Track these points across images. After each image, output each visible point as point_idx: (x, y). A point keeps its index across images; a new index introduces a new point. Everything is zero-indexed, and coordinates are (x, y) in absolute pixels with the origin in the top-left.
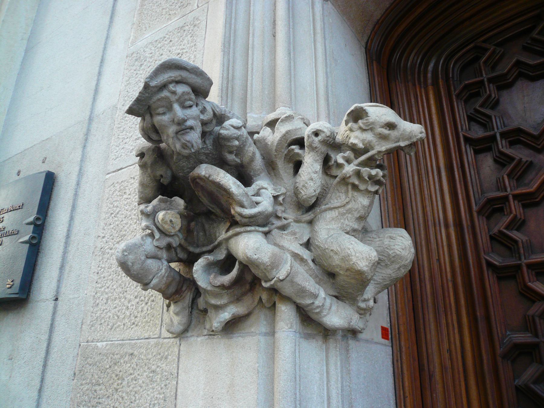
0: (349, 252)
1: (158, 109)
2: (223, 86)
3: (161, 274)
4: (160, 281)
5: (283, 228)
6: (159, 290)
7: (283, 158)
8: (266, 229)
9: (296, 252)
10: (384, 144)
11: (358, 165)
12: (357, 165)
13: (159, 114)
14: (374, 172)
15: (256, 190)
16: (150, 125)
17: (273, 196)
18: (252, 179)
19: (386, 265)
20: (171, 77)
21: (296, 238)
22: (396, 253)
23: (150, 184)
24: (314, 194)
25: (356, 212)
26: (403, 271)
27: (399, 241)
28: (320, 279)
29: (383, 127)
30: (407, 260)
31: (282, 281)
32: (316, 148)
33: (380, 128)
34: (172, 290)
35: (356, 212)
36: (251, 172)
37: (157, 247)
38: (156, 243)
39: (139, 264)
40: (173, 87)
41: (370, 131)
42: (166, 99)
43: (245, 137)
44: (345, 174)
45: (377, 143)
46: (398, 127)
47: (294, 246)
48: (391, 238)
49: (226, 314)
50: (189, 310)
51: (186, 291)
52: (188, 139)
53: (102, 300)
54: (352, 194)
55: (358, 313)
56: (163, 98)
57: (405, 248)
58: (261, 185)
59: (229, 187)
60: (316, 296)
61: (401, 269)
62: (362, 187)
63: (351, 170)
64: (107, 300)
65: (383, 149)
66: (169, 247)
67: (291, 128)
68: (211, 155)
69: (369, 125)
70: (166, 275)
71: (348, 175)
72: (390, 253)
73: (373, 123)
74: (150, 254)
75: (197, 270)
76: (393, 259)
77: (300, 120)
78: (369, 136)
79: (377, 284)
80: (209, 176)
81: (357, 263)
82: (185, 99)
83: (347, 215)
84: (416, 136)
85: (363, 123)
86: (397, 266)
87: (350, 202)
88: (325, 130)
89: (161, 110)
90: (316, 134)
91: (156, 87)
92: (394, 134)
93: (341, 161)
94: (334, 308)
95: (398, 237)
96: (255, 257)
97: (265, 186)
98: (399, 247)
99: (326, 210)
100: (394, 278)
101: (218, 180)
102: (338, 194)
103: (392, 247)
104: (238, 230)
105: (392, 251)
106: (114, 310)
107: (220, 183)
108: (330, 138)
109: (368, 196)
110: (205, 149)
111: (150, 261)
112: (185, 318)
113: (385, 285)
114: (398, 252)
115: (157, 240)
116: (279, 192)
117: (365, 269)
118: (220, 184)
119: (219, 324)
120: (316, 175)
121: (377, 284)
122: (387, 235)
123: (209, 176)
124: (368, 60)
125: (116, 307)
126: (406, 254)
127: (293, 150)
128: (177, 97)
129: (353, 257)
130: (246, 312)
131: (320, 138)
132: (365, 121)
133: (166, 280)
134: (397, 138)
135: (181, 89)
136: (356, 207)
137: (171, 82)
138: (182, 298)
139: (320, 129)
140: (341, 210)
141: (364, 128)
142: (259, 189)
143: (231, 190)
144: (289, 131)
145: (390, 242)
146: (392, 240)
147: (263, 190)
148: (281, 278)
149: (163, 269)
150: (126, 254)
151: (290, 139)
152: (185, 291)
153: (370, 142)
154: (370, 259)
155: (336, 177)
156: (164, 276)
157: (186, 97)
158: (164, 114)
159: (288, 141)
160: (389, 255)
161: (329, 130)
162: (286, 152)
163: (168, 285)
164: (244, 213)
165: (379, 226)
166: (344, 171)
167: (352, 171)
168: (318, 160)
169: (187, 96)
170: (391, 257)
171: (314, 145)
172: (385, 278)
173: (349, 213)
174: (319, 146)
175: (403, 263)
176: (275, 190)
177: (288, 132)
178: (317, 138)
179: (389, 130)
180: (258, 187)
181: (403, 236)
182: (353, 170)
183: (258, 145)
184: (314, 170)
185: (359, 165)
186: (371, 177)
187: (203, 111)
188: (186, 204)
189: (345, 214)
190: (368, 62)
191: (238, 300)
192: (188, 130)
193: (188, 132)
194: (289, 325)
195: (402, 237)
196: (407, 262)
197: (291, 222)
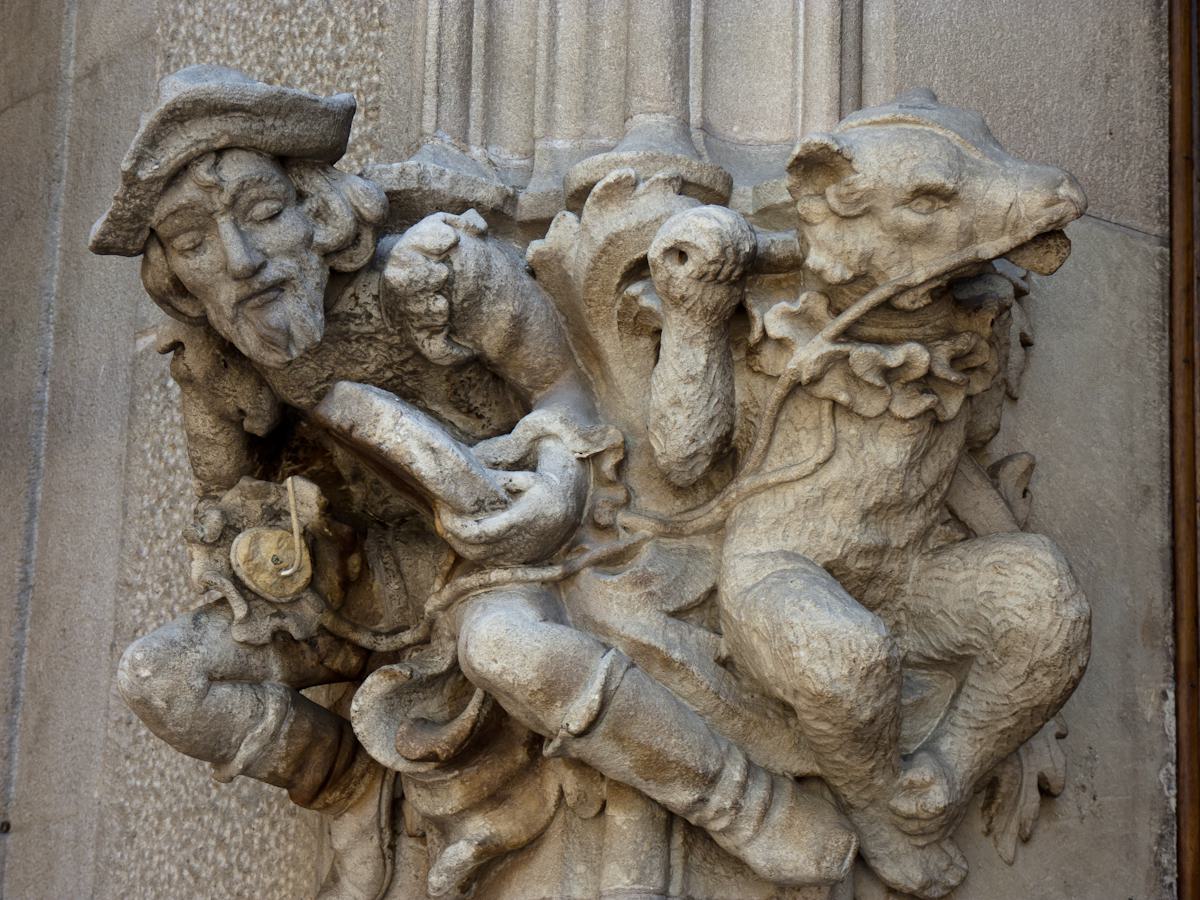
0: (792, 638)
1: (175, 236)
2: (446, 46)
3: (264, 729)
4: (267, 749)
5: (612, 562)
6: (274, 779)
7: (615, 322)
8: (556, 572)
9: (645, 639)
11: (835, 340)
12: (835, 340)
13: (183, 252)
14: (895, 357)
15: (525, 443)
16: (167, 281)
17: (579, 459)
18: (530, 396)
19: (989, 663)
20: (199, 142)
21: (651, 594)
22: (1010, 623)
23: (216, 434)
24: (693, 449)
26: (1048, 682)
27: (1020, 579)
28: (748, 721)
29: (905, 203)
30: (1047, 646)
31: (582, 734)
32: (683, 299)
33: (895, 206)
34: (311, 778)
36: (517, 375)
37: (245, 643)
38: (239, 634)
39: (187, 701)
40: (208, 172)
42: (193, 208)
43: (471, 275)
44: (797, 373)
45: (896, 256)
47: (643, 621)
48: (997, 567)
49: (462, 844)
50: (381, 839)
51: (367, 779)
52: (273, 324)
53: (146, 819)
54: (836, 433)
55: (899, 830)
56: (184, 208)
57: (1037, 602)
58: (539, 426)
59: (407, 459)
60: (710, 780)
61: (1038, 675)
62: (872, 405)
63: (814, 357)
64: (160, 816)
65: (920, 276)
66: (281, 639)
67: (622, 227)
68: (380, 337)
69: (858, 201)
70: (285, 728)
71: (805, 377)
72: (994, 624)
73: (870, 194)
74: (220, 670)
75: (361, 712)
76: (1003, 643)
77: (661, 186)
78: (865, 237)
79: (977, 729)
80: (352, 428)
81: (812, 670)
82: (252, 200)
83: (829, 503)
84: (1030, 219)
85: (839, 196)
86: (1023, 667)
88: (703, 241)
89: (184, 241)
90: (680, 253)
91: (152, 181)
92: (950, 220)
93: (777, 328)
94: (779, 814)
95: (1018, 568)
96: (495, 668)
97: (555, 427)
98: (1020, 601)
99: (754, 492)
100: (1026, 709)
101: (375, 440)
102: (793, 436)
103: (999, 603)
104: (464, 582)
105: (998, 617)
106: (184, 852)
107: (383, 447)
108: (723, 264)
110: (358, 321)
111: (223, 691)
112: (369, 865)
113: (1002, 732)
114: (1016, 621)
115: (242, 622)
116: (598, 445)
117: (841, 687)
118: (381, 451)
119: (444, 878)
120: (691, 389)
121: (977, 729)
122: (987, 560)
123: (352, 428)
125: (186, 844)
126: (1044, 625)
127: (635, 298)
128: (226, 198)
129: (802, 653)
130: (524, 838)
131: (690, 267)
132: (844, 191)
133: (288, 745)
134: (964, 234)
135: (236, 170)
137: (200, 156)
138: (355, 797)
139: (686, 238)
140: (801, 489)
142: (538, 439)
143: (414, 467)
144: (617, 235)
145: (993, 583)
146: (1001, 578)
147: (548, 444)
148: (574, 728)
149: (271, 712)
150: (145, 673)
151: (625, 263)
152: (363, 776)
153: (867, 258)
154: (854, 656)
155: (775, 378)
156: (275, 736)
157: (253, 193)
158: (197, 248)
159: (621, 270)
160: (991, 631)
161: (716, 238)
162: (618, 306)
163: (300, 764)
164: (465, 533)
165: (1147, 490)
166: (791, 365)
167: (816, 362)
168: (696, 336)
169: (255, 190)
170: (997, 636)
171: (677, 293)
172: (997, 708)
173: (835, 497)
174: (691, 292)
175: (1037, 656)
176: (585, 437)
177: (613, 241)
178: (682, 268)
180: (530, 435)
181: (1036, 563)
183: (544, 276)
184: (682, 374)
185: (848, 334)
186: (887, 373)
187: (321, 214)
188: (323, 499)
191: (493, 799)
192: (272, 295)
193: (275, 299)
194: (634, 874)
195: (1028, 564)
196: (1049, 653)
197: (646, 539)
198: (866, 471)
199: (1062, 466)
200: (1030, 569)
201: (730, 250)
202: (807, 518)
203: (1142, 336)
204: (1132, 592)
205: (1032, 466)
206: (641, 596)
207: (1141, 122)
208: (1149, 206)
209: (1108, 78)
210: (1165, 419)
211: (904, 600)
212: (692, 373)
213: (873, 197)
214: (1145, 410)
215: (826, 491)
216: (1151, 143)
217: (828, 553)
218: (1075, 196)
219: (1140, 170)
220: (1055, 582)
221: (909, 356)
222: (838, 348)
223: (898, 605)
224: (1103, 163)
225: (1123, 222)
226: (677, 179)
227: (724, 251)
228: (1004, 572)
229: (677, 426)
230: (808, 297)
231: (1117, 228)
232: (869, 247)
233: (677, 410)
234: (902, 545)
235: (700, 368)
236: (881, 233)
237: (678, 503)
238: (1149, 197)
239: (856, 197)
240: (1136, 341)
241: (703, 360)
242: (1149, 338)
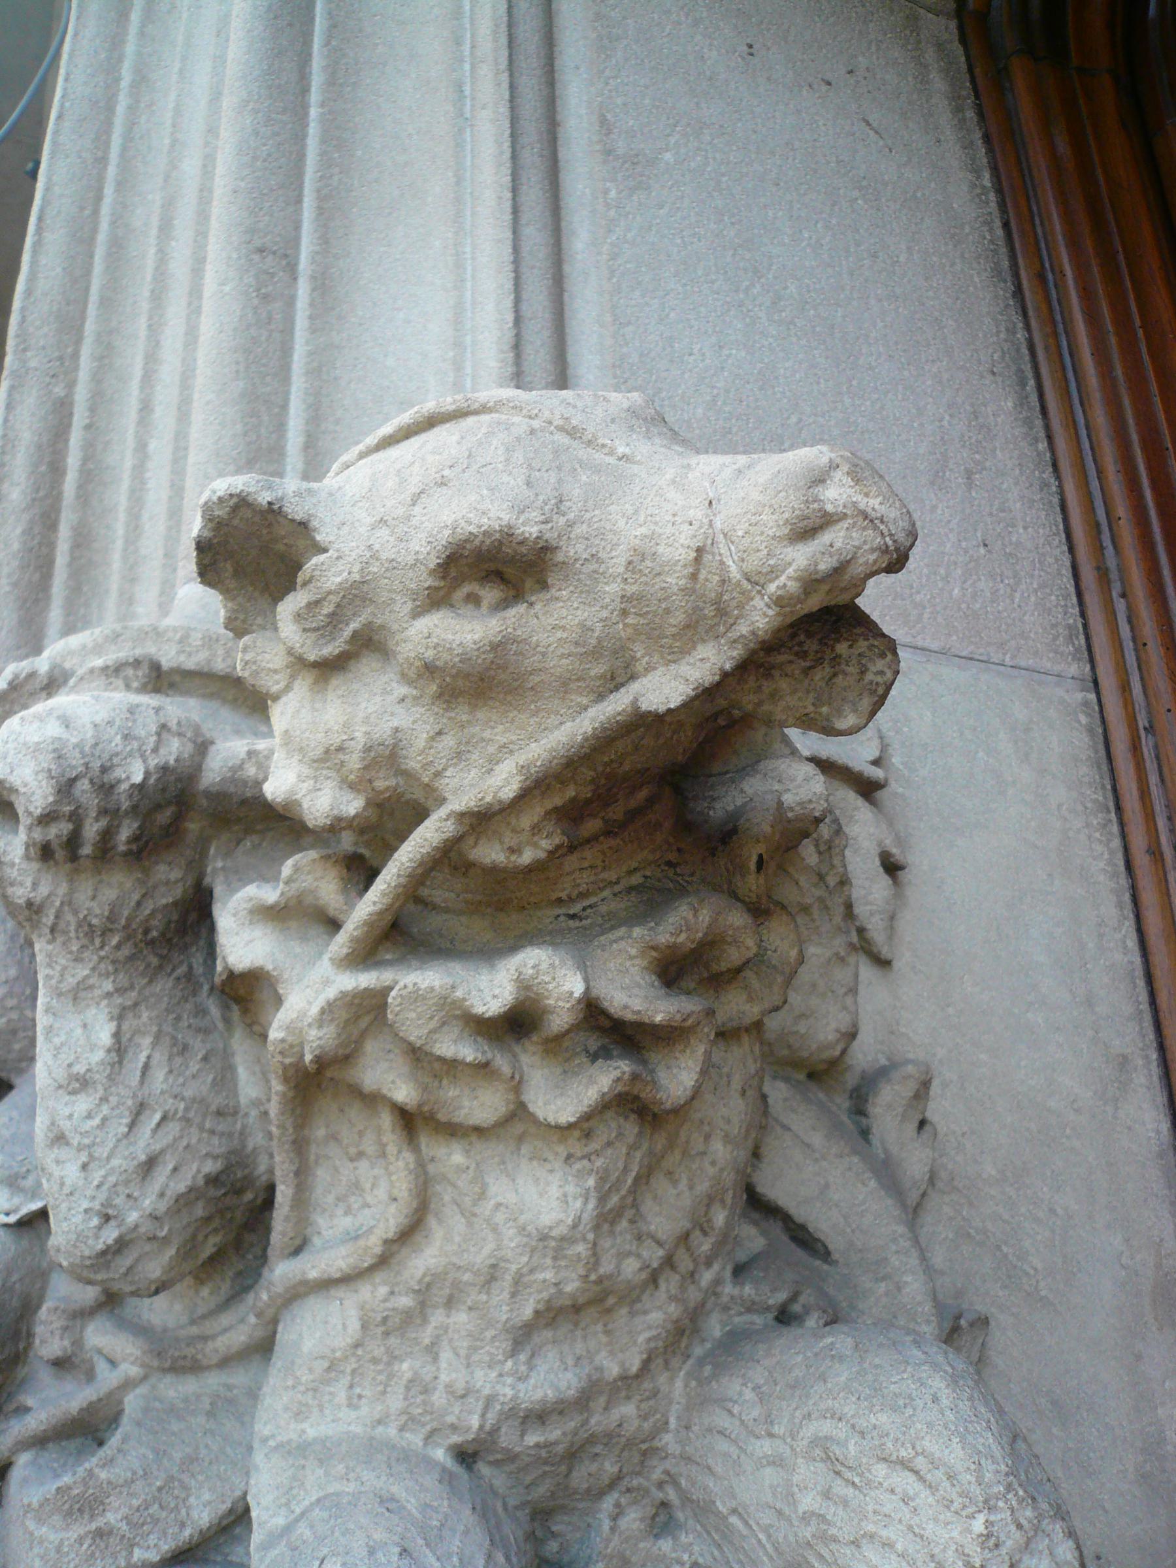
10: (500, 734)
21: (100, 1534)
24: (110, 1235)
25: (501, 1293)
27: (890, 1504)
33: (416, 614)
35: (501, 1293)
41: (367, 665)
45: (449, 742)
46: (573, 550)
69: (335, 620)
83: (437, 1317)
84: (756, 580)
87: (432, 1222)
102: (346, 1170)
109: (562, 1150)
120: (83, 1103)
124: (978, 71)
134: (595, 653)
136: (480, 1257)
141: (330, 650)
146: (840, 1488)
165: (1124, 1062)
167: (320, 1022)
174: (44, 890)
179: (503, 604)
181: (920, 1463)
182: (328, 1010)
189: (411, 1319)
190: (980, 81)
195: (904, 1464)
198: (499, 1248)
199: (983, 1057)
200: (911, 1478)
201: (84, 785)
202: (393, 1358)
203: (1078, 823)
204: (1127, 1240)
205: (926, 1084)
206: (80, 1540)
207: (1025, 528)
208: (1055, 638)
209: (969, 474)
210: (1132, 943)
211: (668, 1465)
212: (80, 1068)
213: (365, 600)
214: (1101, 936)
215: (424, 1293)
216: (1043, 555)
217: (454, 1428)
218: (874, 502)
219: (1036, 591)
220: (978, 1525)
221: (523, 985)
222: (366, 979)
223: (657, 1475)
224: (982, 585)
225: (1023, 663)
226: (137, 663)
227: (65, 788)
228: (848, 1475)
229: (66, 1190)
230: (297, 869)
231: (1015, 672)
232: (383, 730)
233: (63, 1153)
234: (635, 1367)
235: (99, 1055)
236: (404, 690)
237: (205, 1292)
238: (1054, 626)
239: (327, 609)
240: (1071, 834)
241: (104, 1034)
242: (1088, 825)
